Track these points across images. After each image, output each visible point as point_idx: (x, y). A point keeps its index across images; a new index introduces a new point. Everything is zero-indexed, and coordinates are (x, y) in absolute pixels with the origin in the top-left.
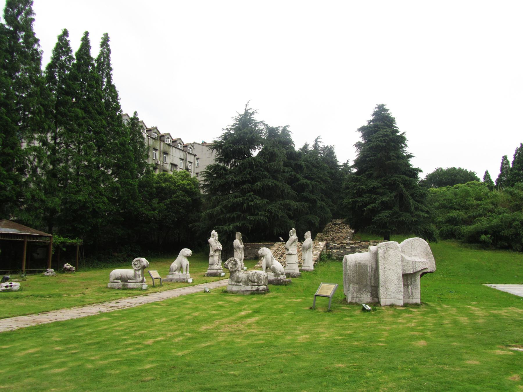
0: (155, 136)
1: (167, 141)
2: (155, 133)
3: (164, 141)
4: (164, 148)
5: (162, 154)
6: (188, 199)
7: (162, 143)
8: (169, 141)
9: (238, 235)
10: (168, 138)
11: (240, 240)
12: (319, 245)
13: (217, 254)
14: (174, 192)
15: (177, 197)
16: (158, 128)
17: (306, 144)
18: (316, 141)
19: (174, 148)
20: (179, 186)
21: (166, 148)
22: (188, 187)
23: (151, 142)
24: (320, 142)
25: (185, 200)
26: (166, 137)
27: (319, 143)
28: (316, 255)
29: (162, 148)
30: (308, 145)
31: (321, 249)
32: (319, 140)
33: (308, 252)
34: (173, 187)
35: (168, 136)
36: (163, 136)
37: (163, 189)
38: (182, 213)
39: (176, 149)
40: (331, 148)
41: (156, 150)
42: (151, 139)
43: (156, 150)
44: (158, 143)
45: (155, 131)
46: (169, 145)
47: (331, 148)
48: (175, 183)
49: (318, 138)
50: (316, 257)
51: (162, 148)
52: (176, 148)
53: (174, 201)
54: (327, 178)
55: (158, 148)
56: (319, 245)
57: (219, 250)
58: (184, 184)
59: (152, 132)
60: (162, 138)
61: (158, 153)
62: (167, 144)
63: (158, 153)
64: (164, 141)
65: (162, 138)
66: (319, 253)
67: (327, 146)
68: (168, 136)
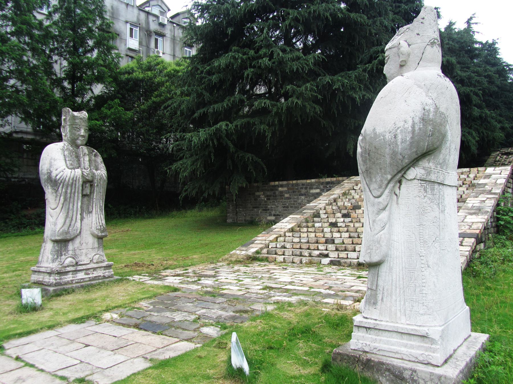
9: (75, 121)
11: (73, 143)
12: (489, 176)
17: (450, 23)
18: (468, 22)
20: (170, 76)
24: (476, 23)
27: (472, 26)
28: (478, 211)
30: (454, 24)
31: (499, 191)
32: (472, 22)
33: (410, 190)
37: (137, 83)
40: (494, 43)
47: (494, 43)
49: (471, 18)
50: (478, 222)
53: (154, 102)
54: (490, 73)
56: (489, 176)
59: (181, 16)
66: (489, 204)
67: (487, 42)
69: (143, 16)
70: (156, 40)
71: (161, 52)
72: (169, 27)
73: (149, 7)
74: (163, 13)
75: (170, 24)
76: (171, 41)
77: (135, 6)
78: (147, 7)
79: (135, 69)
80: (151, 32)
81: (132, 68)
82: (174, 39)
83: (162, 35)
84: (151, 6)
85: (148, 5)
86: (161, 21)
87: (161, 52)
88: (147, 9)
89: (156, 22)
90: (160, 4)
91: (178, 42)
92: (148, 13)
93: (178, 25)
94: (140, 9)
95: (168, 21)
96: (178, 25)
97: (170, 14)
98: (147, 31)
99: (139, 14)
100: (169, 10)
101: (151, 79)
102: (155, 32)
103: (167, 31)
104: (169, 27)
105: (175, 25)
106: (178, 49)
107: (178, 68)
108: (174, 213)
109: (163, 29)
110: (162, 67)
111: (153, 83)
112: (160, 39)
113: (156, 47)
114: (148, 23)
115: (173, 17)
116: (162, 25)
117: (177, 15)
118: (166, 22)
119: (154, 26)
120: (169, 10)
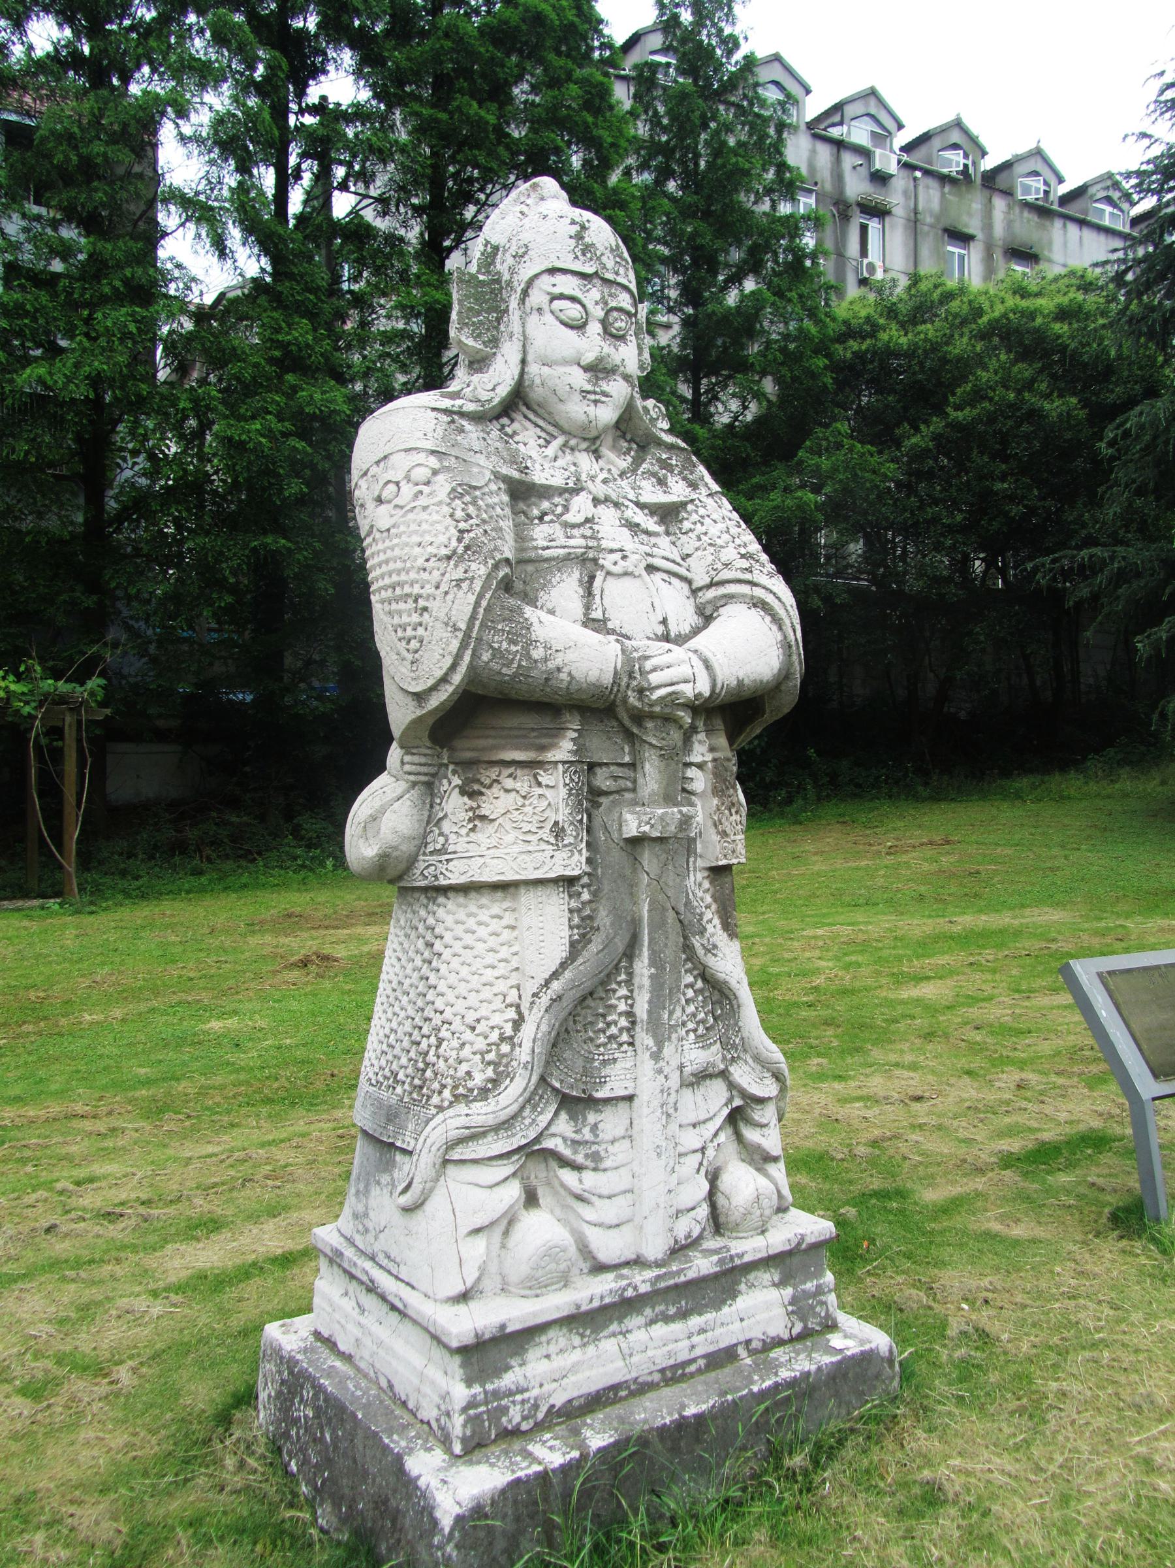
0: (954, 162)
1: (1027, 189)
2: (955, 146)
3: (1008, 193)
4: (1009, 224)
5: (998, 256)
6: (1053, 407)
7: (999, 204)
8: (1031, 188)
10: (1036, 174)
13: (519, 824)
14: (964, 367)
15: (978, 395)
16: (968, 122)
19: (1073, 229)
21: (1027, 228)
22: (1060, 328)
23: (931, 196)
25: (1034, 414)
26: (1021, 169)
29: (999, 230)
34: (961, 345)
35: (1033, 165)
36: (1006, 166)
38: (1011, 498)
39: (1087, 234)
41: (963, 238)
42: (933, 183)
43: (963, 238)
44: (975, 202)
45: (955, 137)
46: (1042, 211)
48: (978, 312)
51: (999, 230)
52: (1082, 223)
53: (955, 426)
55: (973, 226)
57: (612, 713)
58: (1032, 315)
59: (936, 143)
60: (1001, 181)
61: (974, 257)
62: (1026, 205)
63: (974, 257)
64: (1008, 193)
65: (995, 181)
68: (1039, 166)
69: (824, 153)
70: (864, 229)
71: (878, 264)
72: (900, 182)
73: (841, 123)
74: (882, 137)
75: (904, 173)
76: (906, 228)
77: (803, 127)
78: (834, 125)
79: (882, 321)
80: (848, 206)
81: (868, 319)
82: (914, 221)
83: (880, 212)
84: (846, 120)
85: (837, 118)
86: (878, 166)
87: (878, 264)
88: (835, 132)
89: (863, 171)
90: (873, 112)
91: (926, 228)
92: (839, 145)
93: (927, 173)
94: (816, 136)
95: (899, 162)
96: (927, 173)
97: (902, 139)
98: (836, 204)
99: (813, 151)
100: (900, 127)
101: (935, 347)
102: (859, 204)
103: (896, 198)
104: (900, 182)
105: (918, 174)
106: (925, 252)
107: (1024, 304)
108: (1023, 783)
109: (883, 191)
110: (966, 307)
111: (944, 360)
112: (874, 225)
113: (864, 252)
114: (838, 177)
115: (908, 148)
116: (880, 179)
117: (924, 139)
118: (893, 168)
119: (856, 187)
120: (900, 127)
